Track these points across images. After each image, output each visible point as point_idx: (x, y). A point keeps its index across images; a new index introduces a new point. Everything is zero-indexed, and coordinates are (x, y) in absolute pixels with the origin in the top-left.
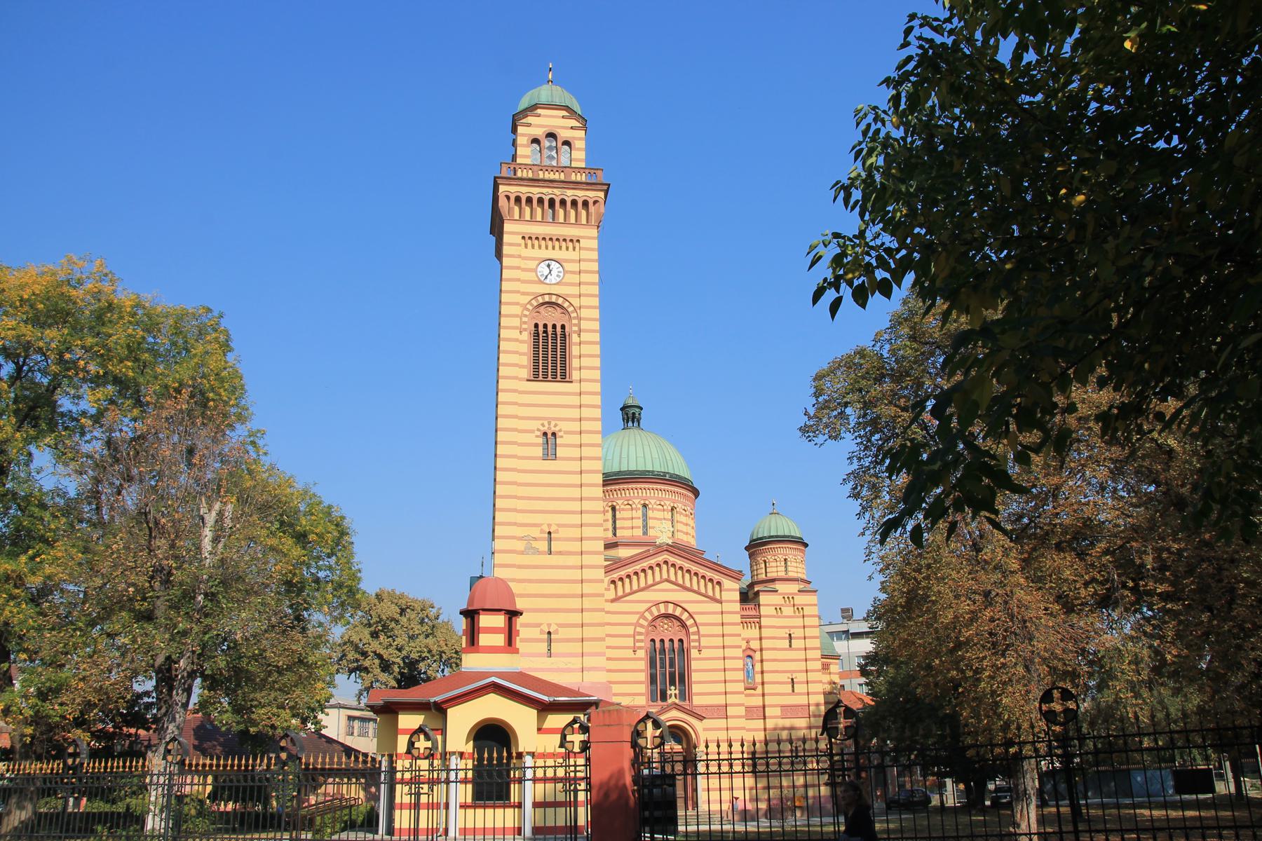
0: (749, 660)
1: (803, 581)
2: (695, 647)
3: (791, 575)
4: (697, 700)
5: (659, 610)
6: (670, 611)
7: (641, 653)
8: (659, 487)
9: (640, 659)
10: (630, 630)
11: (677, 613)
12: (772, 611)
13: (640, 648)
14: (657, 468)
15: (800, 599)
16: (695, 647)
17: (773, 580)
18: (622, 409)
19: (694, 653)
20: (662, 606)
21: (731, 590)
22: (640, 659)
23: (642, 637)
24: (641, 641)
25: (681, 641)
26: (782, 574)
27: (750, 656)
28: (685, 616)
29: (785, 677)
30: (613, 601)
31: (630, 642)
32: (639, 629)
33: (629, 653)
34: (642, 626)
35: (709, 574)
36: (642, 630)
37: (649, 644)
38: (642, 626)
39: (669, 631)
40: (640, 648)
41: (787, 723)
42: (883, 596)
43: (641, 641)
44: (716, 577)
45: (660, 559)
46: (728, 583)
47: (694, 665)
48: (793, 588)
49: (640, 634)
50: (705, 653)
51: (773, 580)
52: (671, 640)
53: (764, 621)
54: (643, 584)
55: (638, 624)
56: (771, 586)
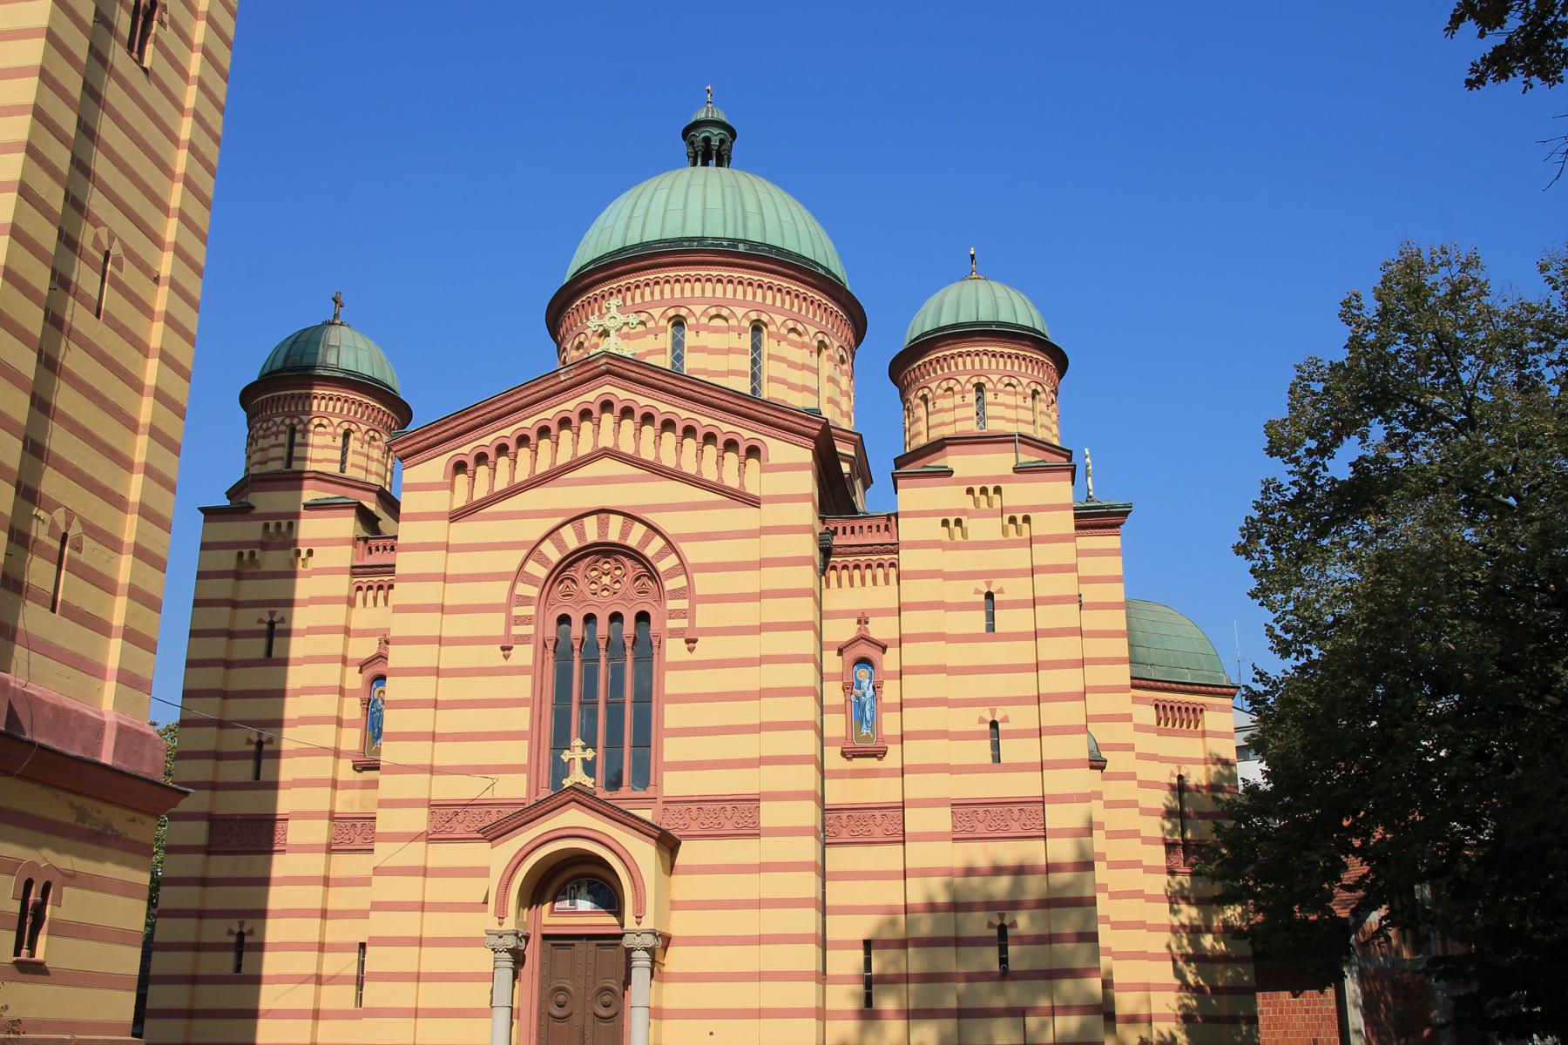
0: (863, 673)
1: (1026, 440)
2: (675, 633)
3: (994, 426)
4: (673, 784)
5: (581, 534)
6: (613, 536)
7: (524, 655)
8: (715, 272)
9: (521, 670)
10: (498, 592)
11: (633, 541)
12: (932, 529)
13: (523, 640)
14: (715, 230)
15: (1020, 493)
16: (675, 633)
17: (939, 445)
18: (686, 132)
19: (674, 649)
20: (591, 524)
21: (788, 471)
22: (521, 670)
23: (530, 611)
24: (525, 620)
25: (643, 617)
26: (970, 427)
27: (864, 661)
28: (653, 548)
29: (972, 720)
30: (456, 516)
31: (495, 624)
32: (523, 589)
33: (493, 656)
34: (531, 580)
35: (663, 407)
36: (533, 591)
37: (551, 631)
38: (531, 580)
39: (603, 591)
40: (523, 640)
41: (981, 854)
42: (1280, 471)
43: (525, 620)
44: (746, 434)
45: (591, 396)
46: (779, 449)
47: (671, 682)
48: (999, 462)
49: (525, 601)
50: (707, 648)
51: (939, 445)
52: (616, 617)
53: (907, 559)
54: (543, 466)
55: (520, 575)
56: (936, 462)
